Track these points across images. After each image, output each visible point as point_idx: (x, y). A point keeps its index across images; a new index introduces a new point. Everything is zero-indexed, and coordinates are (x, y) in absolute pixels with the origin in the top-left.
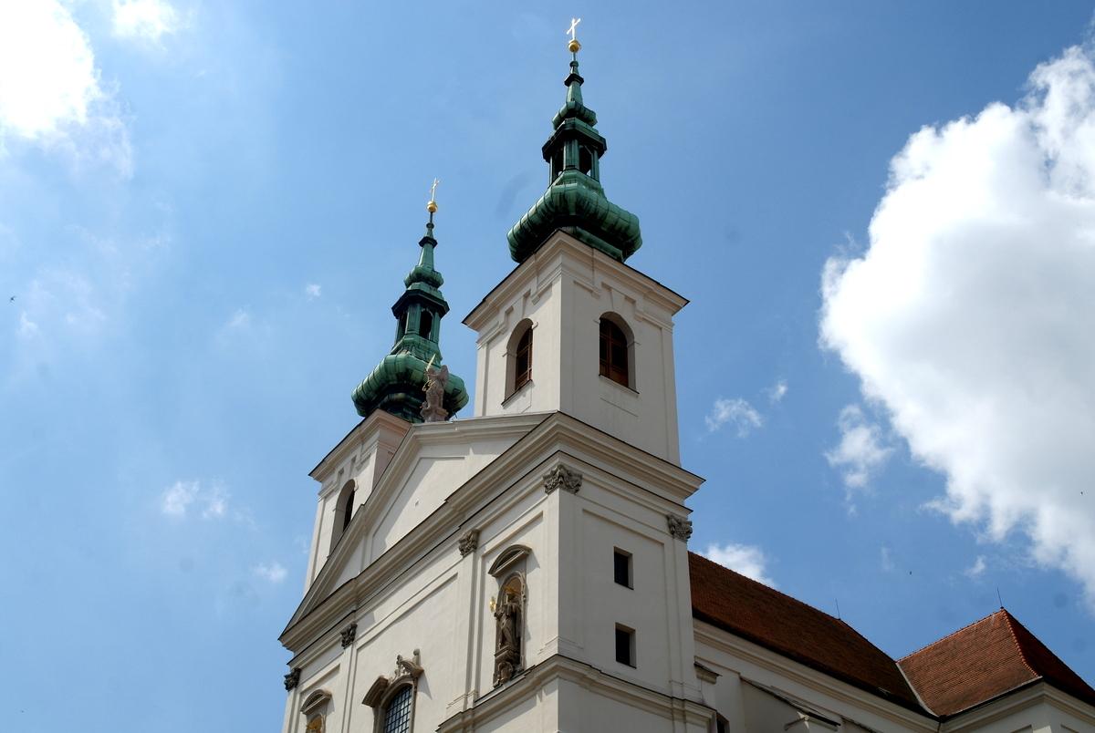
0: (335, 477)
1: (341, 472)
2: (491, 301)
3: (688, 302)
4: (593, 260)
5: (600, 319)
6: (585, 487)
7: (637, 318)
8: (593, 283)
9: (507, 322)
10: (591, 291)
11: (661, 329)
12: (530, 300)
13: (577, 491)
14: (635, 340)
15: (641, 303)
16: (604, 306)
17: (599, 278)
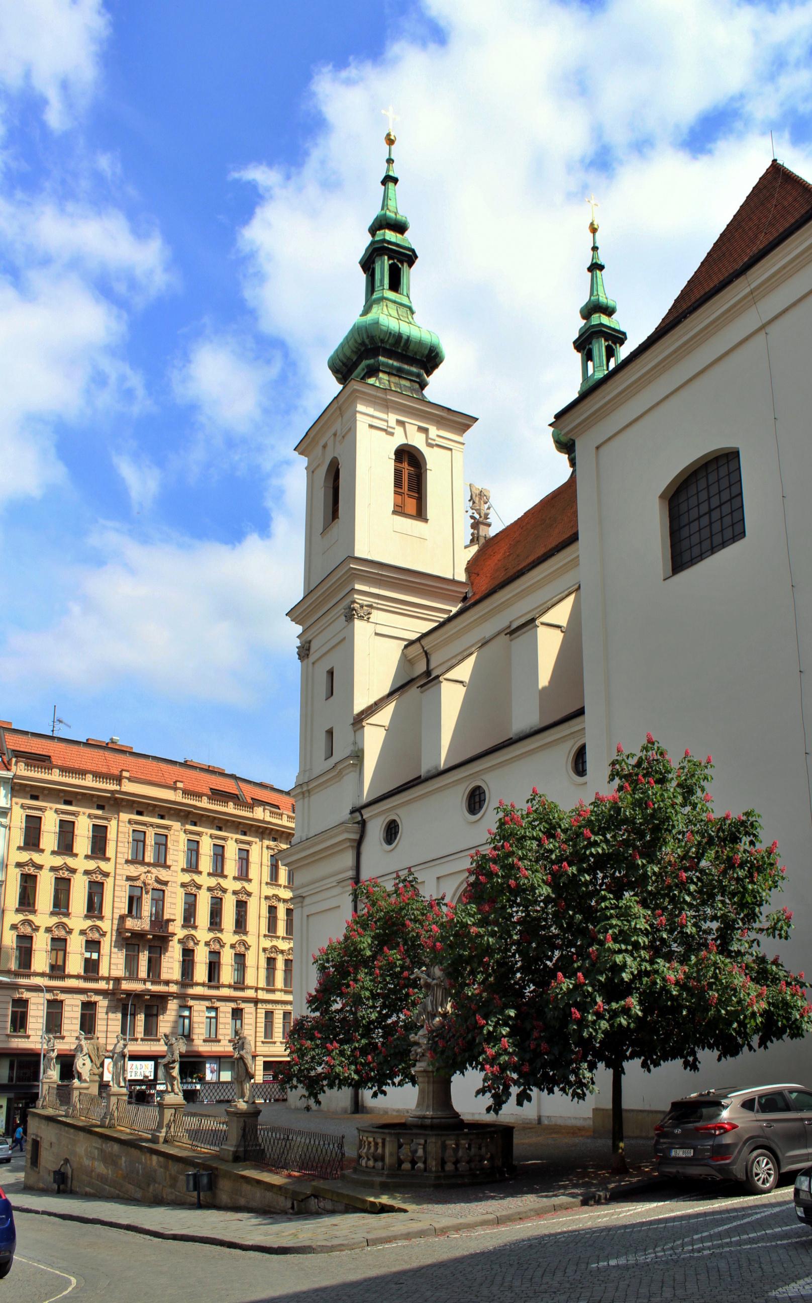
0: (319, 450)
1: (324, 447)
2: (311, 435)
3: (477, 419)
4: (386, 400)
5: (395, 454)
6: (376, 615)
7: (430, 445)
8: (387, 421)
9: (323, 454)
10: (385, 430)
11: (451, 449)
12: (339, 438)
13: (368, 618)
14: (428, 467)
15: (433, 431)
16: (399, 439)
17: (392, 418)
